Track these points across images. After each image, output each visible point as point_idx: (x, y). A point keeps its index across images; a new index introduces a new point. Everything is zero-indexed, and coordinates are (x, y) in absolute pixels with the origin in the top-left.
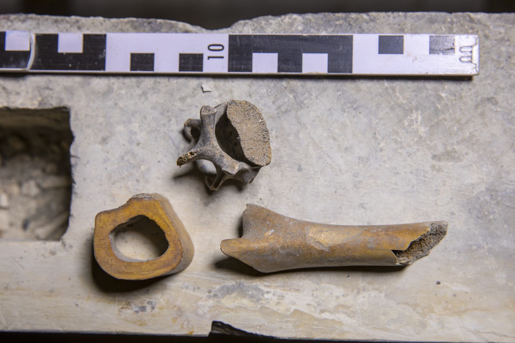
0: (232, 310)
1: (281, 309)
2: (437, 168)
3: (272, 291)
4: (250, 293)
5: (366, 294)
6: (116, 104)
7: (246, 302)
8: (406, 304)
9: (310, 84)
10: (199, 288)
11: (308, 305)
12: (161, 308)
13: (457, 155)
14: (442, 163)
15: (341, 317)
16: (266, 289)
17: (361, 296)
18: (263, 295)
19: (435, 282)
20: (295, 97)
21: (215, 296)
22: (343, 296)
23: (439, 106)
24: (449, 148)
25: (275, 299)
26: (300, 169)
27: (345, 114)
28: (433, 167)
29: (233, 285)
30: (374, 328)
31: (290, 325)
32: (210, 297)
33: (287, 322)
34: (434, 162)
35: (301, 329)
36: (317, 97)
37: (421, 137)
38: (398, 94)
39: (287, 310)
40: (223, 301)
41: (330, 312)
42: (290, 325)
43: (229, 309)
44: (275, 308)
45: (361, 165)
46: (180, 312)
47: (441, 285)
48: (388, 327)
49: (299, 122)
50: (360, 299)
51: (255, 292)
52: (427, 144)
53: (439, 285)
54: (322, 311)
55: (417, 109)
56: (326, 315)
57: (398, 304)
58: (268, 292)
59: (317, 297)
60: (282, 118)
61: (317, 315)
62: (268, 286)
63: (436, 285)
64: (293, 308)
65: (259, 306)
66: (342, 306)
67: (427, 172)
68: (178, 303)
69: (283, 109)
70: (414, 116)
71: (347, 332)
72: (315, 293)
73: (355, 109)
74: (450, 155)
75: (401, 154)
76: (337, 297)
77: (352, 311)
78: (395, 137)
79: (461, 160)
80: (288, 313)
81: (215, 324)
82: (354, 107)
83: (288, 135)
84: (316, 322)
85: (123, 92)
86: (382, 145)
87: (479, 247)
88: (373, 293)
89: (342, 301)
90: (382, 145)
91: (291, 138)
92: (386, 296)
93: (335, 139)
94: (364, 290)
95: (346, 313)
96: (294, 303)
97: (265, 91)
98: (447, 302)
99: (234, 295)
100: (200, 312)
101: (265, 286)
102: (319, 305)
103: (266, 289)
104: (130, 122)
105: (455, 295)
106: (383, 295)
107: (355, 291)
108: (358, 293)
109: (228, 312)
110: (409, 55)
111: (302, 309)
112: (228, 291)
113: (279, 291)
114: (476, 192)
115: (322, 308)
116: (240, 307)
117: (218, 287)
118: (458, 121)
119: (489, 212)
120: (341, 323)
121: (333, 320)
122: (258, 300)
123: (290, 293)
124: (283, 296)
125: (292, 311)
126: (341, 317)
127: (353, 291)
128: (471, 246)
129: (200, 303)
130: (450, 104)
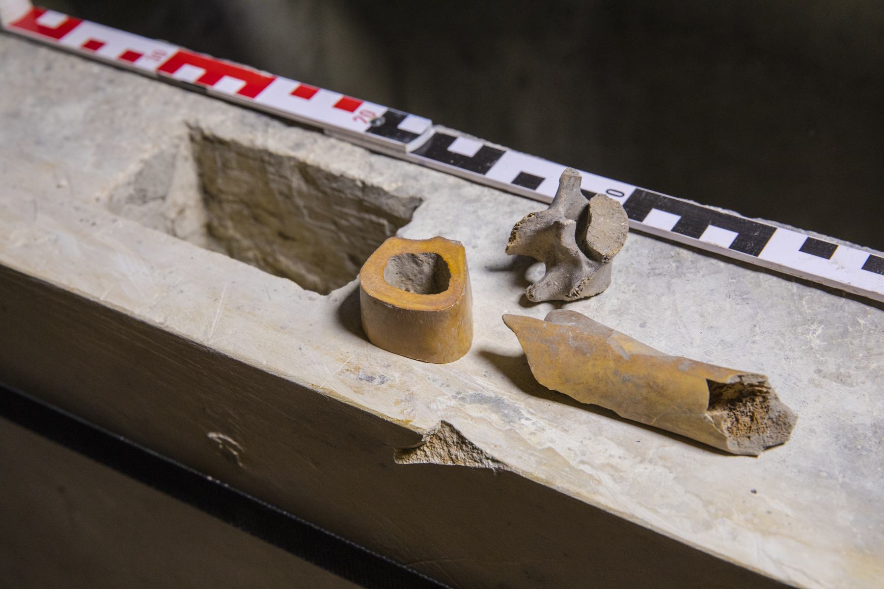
0: (472, 418)
1: (533, 440)
2: (817, 382)
3: (534, 419)
4: (506, 412)
5: (650, 467)
6: (475, 212)
7: (495, 417)
8: (697, 496)
9: (703, 261)
10: (448, 386)
11: (569, 449)
12: (390, 386)
13: (849, 381)
14: (825, 381)
15: (605, 478)
16: (529, 416)
17: (642, 466)
18: (520, 419)
19: (750, 490)
20: (678, 267)
21: (463, 399)
22: (620, 458)
23: (850, 329)
24: (842, 370)
25: (532, 428)
26: (643, 325)
27: (728, 300)
28: (811, 381)
29: (490, 398)
30: (639, 503)
31: (533, 459)
32: (454, 397)
33: (532, 455)
34: (816, 376)
35: (544, 467)
36: (703, 276)
37: (811, 348)
38: (804, 302)
39: (540, 444)
40: (467, 406)
41: (592, 466)
42: (533, 459)
43: (470, 416)
44: (526, 437)
45: (720, 347)
46: (411, 397)
47: (757, 495)
48: (659, 510)
49: (669, 288)
50: (640, 468)
51: (512, 413)
52: (816, 357)
53: (753, 494)
54: (583, 462)
55: (821, 322)
56: (586, 468)
57: (686, 492)
58: (527, 419)
59: (586, 446)
60: (651, 278)
61: (573, 463)
62: (532, 414)
63: (750, 492)
64: (549, 445)
65: (508, 427)
66: (612, 467)
67: (800, 381)
68: (413, 389)
69: (657, 271)
70: (813, 327)
71: (601, 494)
72: (585, 442)
73: (743, 299)
74: (840, 378)
75: (776, 355)
76: (611, 456)
77: (621, 477)
78: (778, 337)
79: (851, 385)
80: (539, 447)
81: (444, 423)
82: (744, 297)
83: (648, 294)
84: (568, 469)
85: (490, 205)
86: (757, 338)
87: (831, 476)
88: (660, 470)
89: (615, 461)
90: (757, 338)
91: (650, 297)
92: (675, 478)
93: (702, 316)
94: (650, 461)
95: (612, 476)
96: (552, 441)
97: (647, 252)
98: (754, 515)
99: (485, 406)
100: (433, 406)
101: (529, 412)
102: (583, 454)
103: (529, 416)
104: (479, 228)
105: (769, 512)
106: (672, 476)
107: (639, 458)
108: (641, 462)
109: (467, 419)
110: (836, 262)
111: (558, 450)
112: (480, 399)
113: (542, 423)
114: (855, 421)
115: (584, 458)
116: (484, 420)
117: (471, 392)
118: (868, 350)
119: (863, 447)
120: (599, 482)
121: (591, 476)
122: (510, 422)
123: (554, 430)
124: (543, 430)
125: (545, 446)
126: (605, 478)
127: (636, 457)
128: (820, 471)
129: (440, 398)
130: (865, 332)
